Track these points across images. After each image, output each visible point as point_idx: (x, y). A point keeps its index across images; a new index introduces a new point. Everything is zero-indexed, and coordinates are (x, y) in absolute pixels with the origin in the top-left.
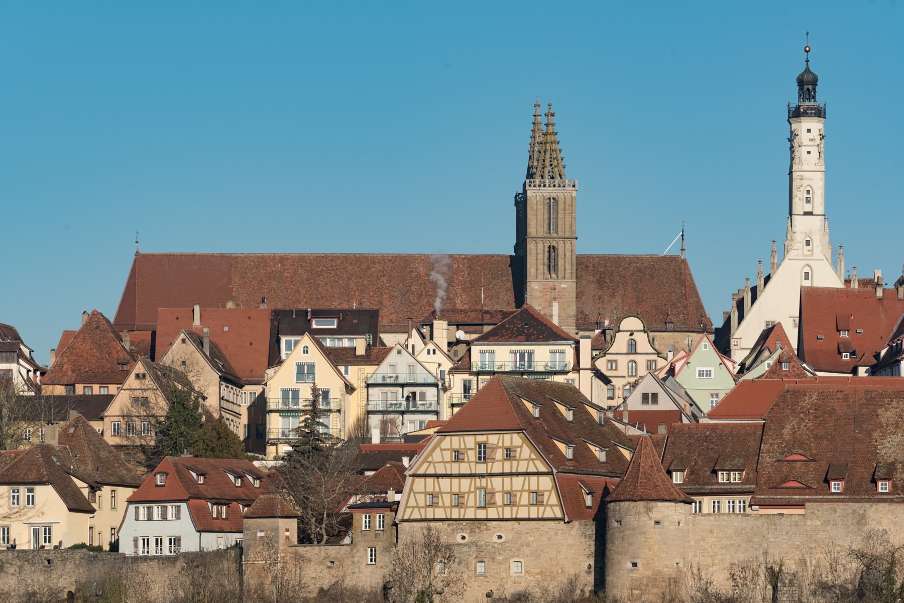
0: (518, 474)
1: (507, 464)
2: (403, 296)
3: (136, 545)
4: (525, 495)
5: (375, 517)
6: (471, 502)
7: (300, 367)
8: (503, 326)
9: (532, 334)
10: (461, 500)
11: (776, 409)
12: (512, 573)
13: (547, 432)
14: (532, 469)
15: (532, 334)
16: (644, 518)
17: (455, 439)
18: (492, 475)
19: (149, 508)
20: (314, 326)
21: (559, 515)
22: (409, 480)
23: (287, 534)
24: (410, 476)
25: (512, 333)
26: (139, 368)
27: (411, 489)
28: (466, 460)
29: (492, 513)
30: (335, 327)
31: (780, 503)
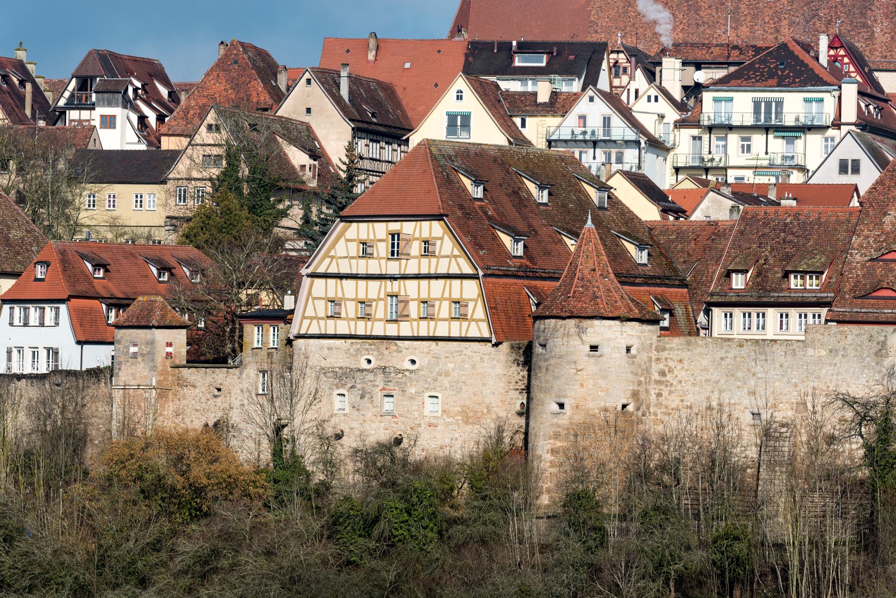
0: (437, 277)
1: (425, 261)
2: (807, 22)
3: (9, 359)
4: (446, 304)
5: (268, 331)
6: (380, 314)
7: (452, 118)
8: (752, 65)
9: (788, 76)
10: (368, 310)
11: (879, 188)
12: (426, 412)
13: (490, 218)
14: (454, 270)
15: (788, 76)
16: (575, 342)
17: (363, 226)
18: (405, 277)
19: (25, 309)
20: (518, 62)
21: (486, 334)
22: (306, 281)
23: (169, 349)
24: (308, 276)
25: (762, 75)
26: (211, 118)
27: (310, 293)
28: (375, 255)
29: (405, 329)
30: (544, 64)
31: (865, 318)
